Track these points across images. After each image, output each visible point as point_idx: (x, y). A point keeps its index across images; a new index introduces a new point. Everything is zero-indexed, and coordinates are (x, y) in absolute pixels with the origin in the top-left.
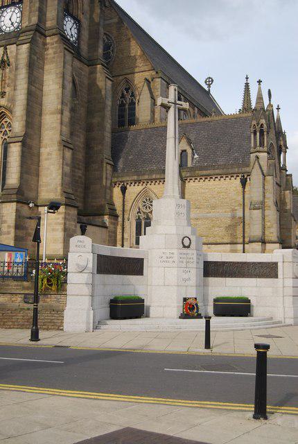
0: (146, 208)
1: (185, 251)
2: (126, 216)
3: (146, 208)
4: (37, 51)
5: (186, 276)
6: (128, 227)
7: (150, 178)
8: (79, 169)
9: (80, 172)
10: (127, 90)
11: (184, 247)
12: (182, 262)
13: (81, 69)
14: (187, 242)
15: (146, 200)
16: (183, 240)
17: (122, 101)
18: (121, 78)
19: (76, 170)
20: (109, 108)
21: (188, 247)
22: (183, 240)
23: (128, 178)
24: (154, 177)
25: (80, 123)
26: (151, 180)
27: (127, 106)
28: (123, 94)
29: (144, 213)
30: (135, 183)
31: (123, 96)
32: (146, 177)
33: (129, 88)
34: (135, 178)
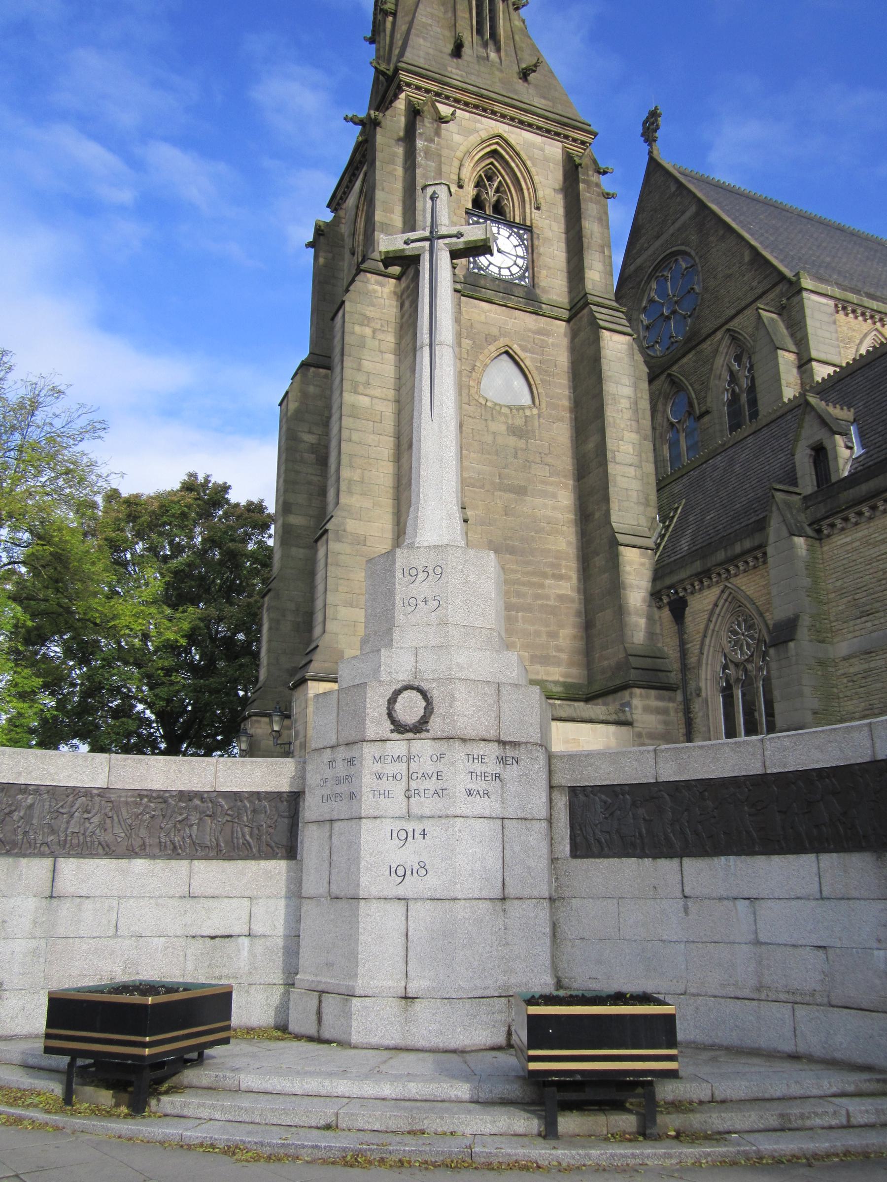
0: (741, 649)
1: (398, 746)
2: (692, 685)
3: (741, 649)
4: (368, 314)
5: (408, 856)
6: (700, 714)
7: (730, 553)
8: (560, 577)
9: (563, 583)
10: (738, 359)
11: (399, 727)
12: (387, 794)
13: (540, 332)
14: (410, 708)
15: (739, 625)
16: (392, 701)
17: (733, 392)
18: (719, 335)
19: (547, 582)
20: (624, 404)
21: (420, 727)
22: (392, 701)
23: (683, 574)
24: (738, 549)
25: (549, 460)
26: (733, 560)
27: (744, 398)
28: (732, 373)
29: (737, 665)
30: (701, 582)
31: (733, 378)
32: (721, 556)
33: (742, 353)
34: (698, 566)
